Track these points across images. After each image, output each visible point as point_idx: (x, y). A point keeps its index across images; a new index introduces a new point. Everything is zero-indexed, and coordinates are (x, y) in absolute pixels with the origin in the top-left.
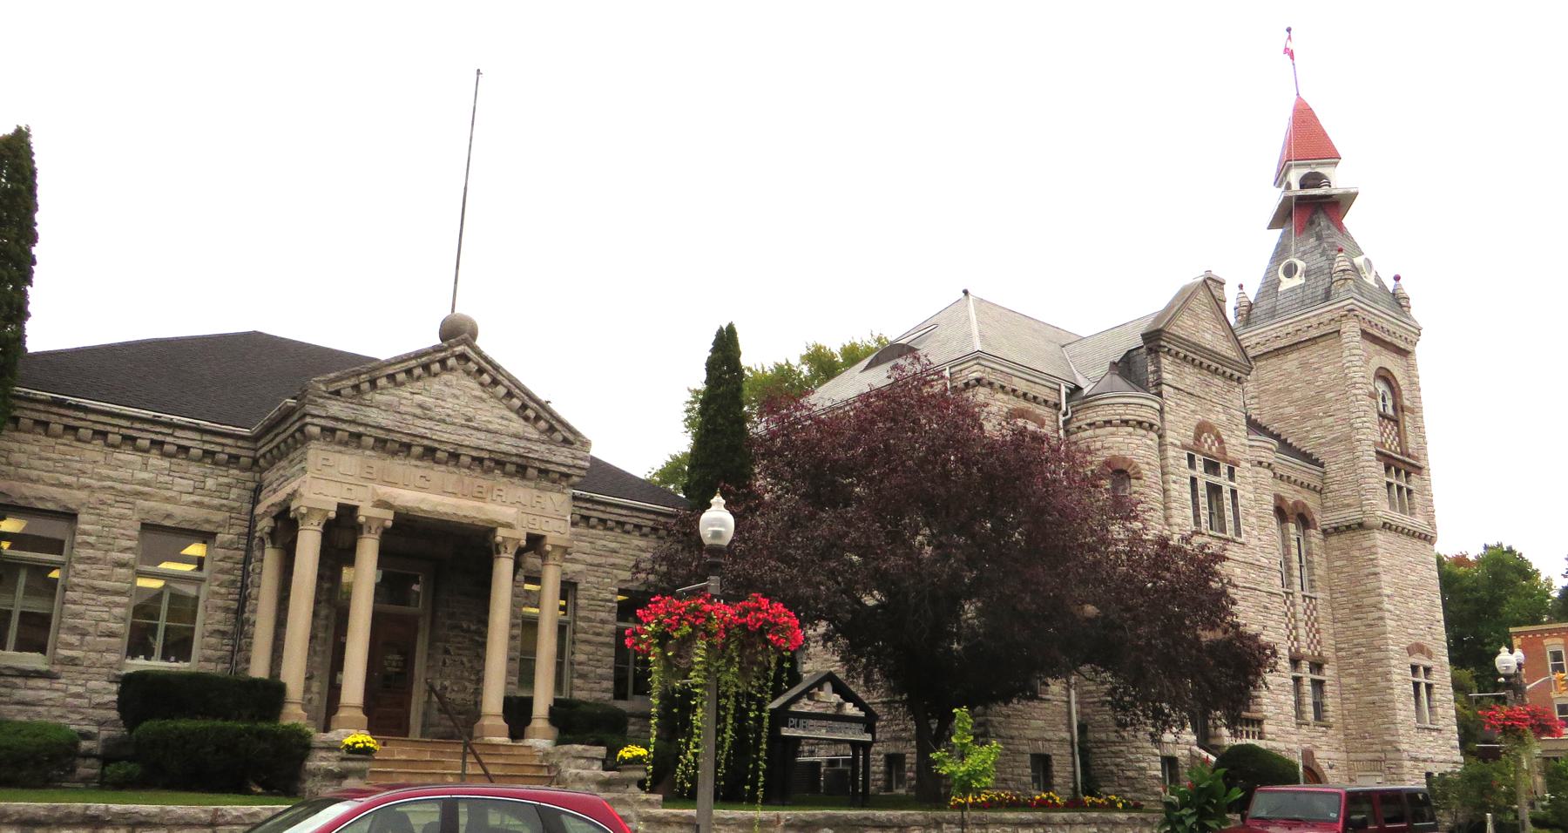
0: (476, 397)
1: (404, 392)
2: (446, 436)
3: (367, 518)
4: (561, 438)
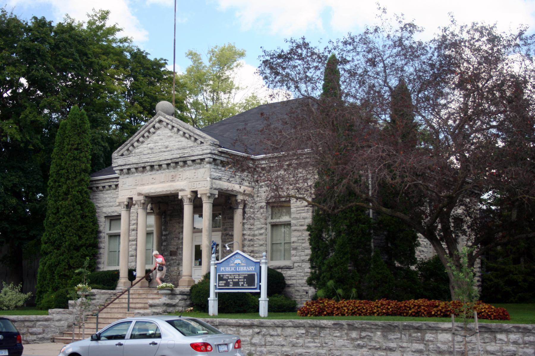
0: (169, 136)
1: (144, 145)
2: (154, 159)
3: (136, 201)
4: (200, 142)
